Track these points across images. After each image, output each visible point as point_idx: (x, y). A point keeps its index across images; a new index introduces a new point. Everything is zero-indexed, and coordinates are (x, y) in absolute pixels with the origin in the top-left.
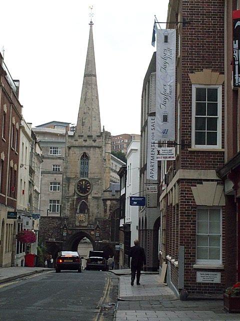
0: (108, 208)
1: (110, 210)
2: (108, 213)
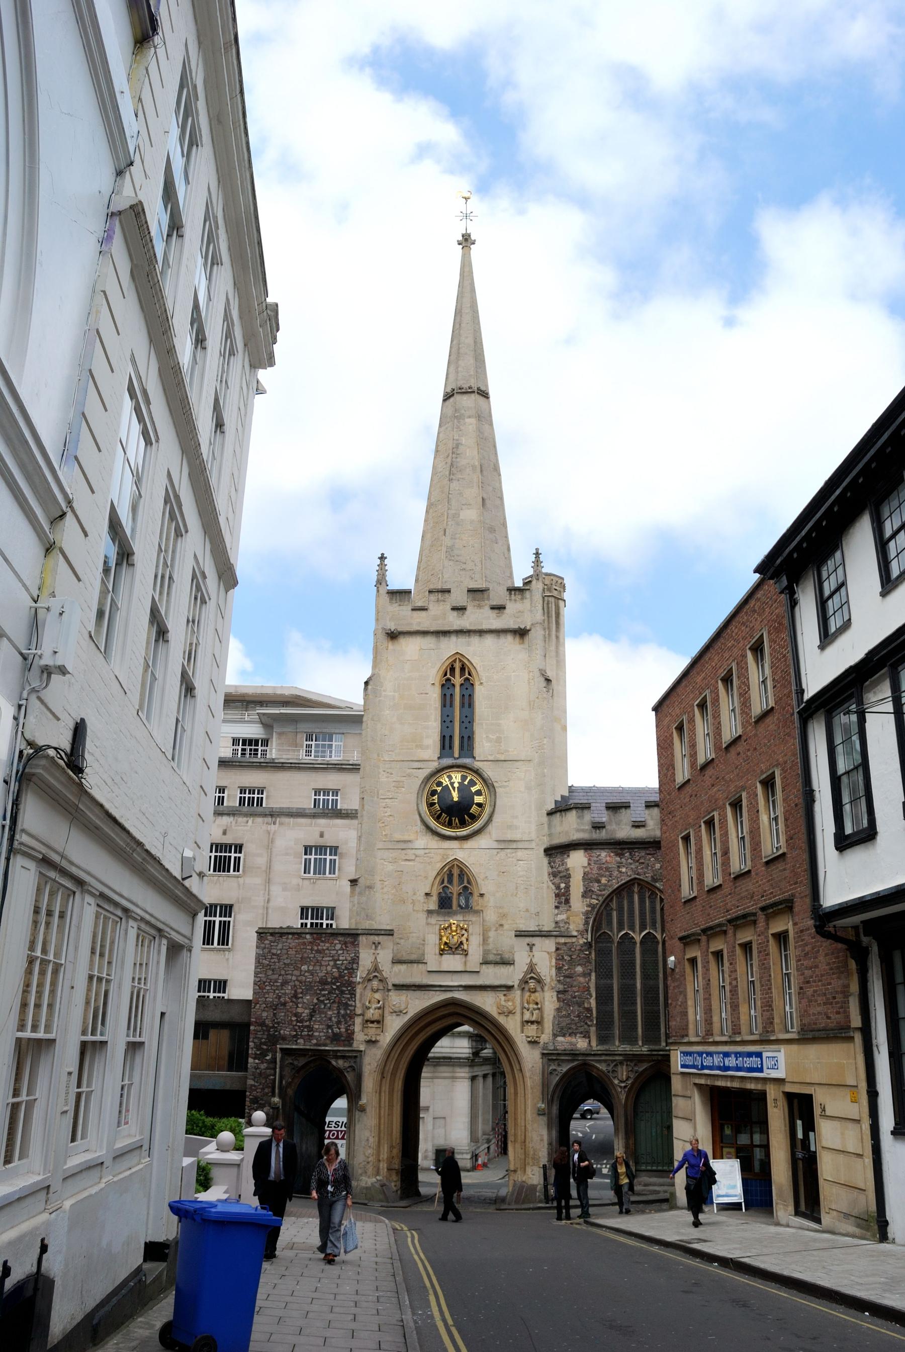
0: (577, 887)
1: (585, 895)
2: (579, 905)
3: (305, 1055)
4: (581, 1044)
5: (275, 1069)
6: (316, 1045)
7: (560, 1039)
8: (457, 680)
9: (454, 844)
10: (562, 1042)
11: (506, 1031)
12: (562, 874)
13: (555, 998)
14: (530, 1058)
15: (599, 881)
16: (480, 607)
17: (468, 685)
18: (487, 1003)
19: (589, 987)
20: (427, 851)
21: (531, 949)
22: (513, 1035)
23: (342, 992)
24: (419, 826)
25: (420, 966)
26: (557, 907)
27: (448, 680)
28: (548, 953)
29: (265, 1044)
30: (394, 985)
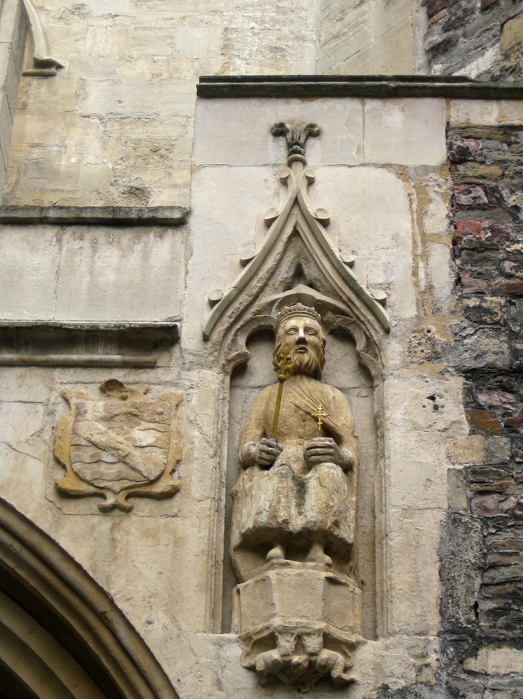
11: (106, 613)
13: (454, 411)
21: (295, 153)
22: (153, 637)
28: (402, 172)
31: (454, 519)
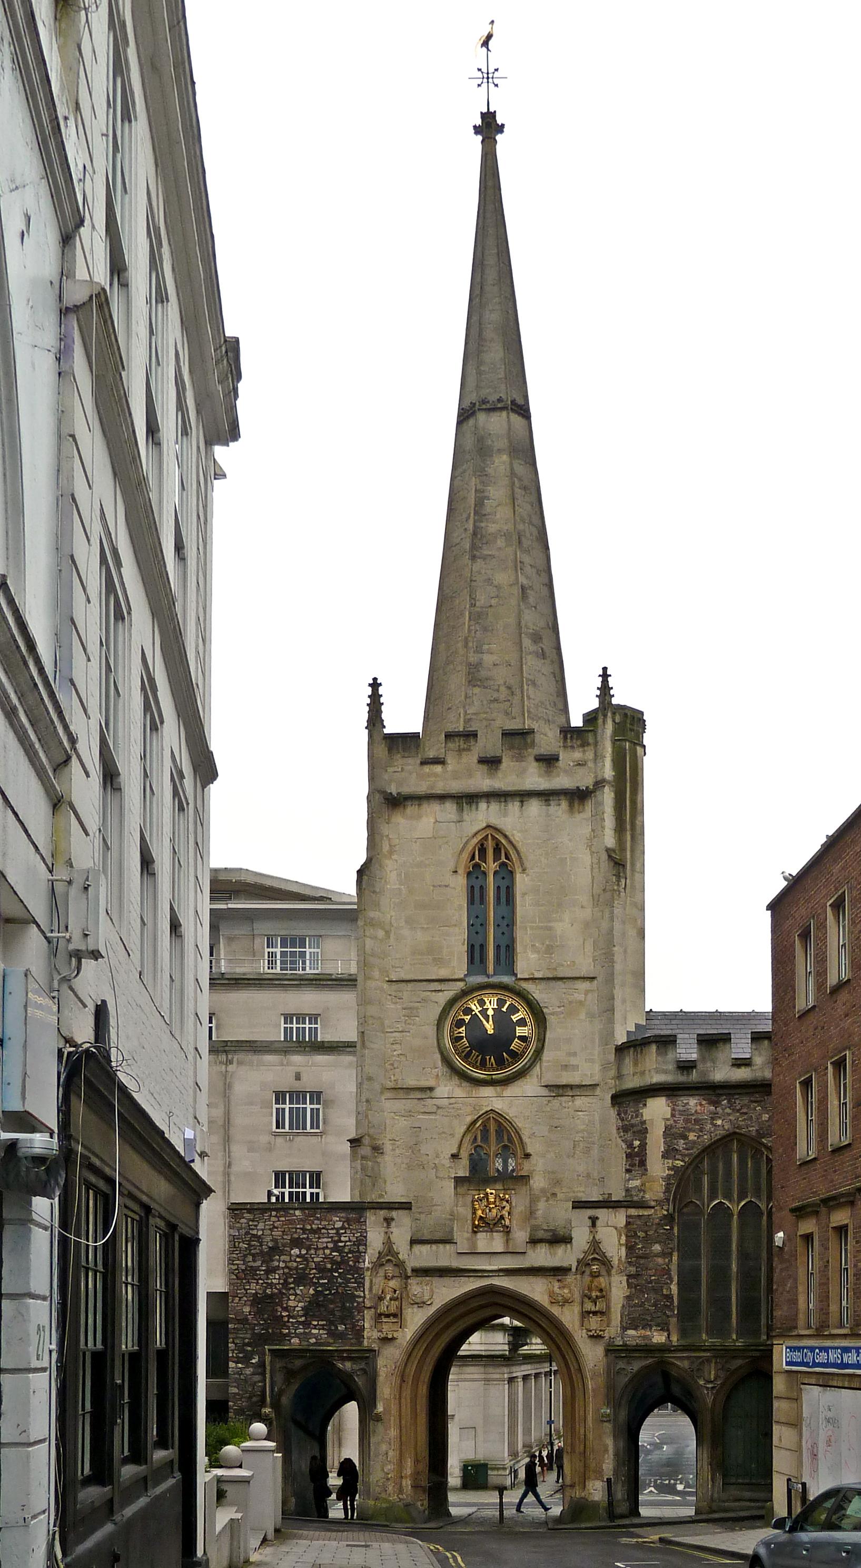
0: (656, 1143)
1: (665, 1155)
2: (658, 1168)
3: (302, 1357)
4: (659, 1338)
5: (263, 1374)
6: (313, 1344)
7: (631, 1332)
8: (491, 866)
9: (488, 1091)
10: (633, 1337)
12: (635, 1129)
13: (625, 1284)
14: (592, 1356)
15: (685, 1137)
16: (520, 758)
17: (506, 873)
18: (536, 1290)
19: (669, 1270)
20: (453, 1100)
23: (348, 1281)
24: (441, 1068)
25: (448, 1246)
26: (628, 1171)
27: (477, 866)
28: (616, 1228)
29: (248, 1344)
30: (413, 1270)
31: (623, 1306)
